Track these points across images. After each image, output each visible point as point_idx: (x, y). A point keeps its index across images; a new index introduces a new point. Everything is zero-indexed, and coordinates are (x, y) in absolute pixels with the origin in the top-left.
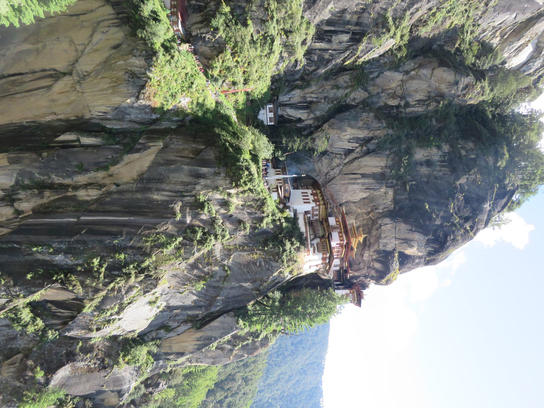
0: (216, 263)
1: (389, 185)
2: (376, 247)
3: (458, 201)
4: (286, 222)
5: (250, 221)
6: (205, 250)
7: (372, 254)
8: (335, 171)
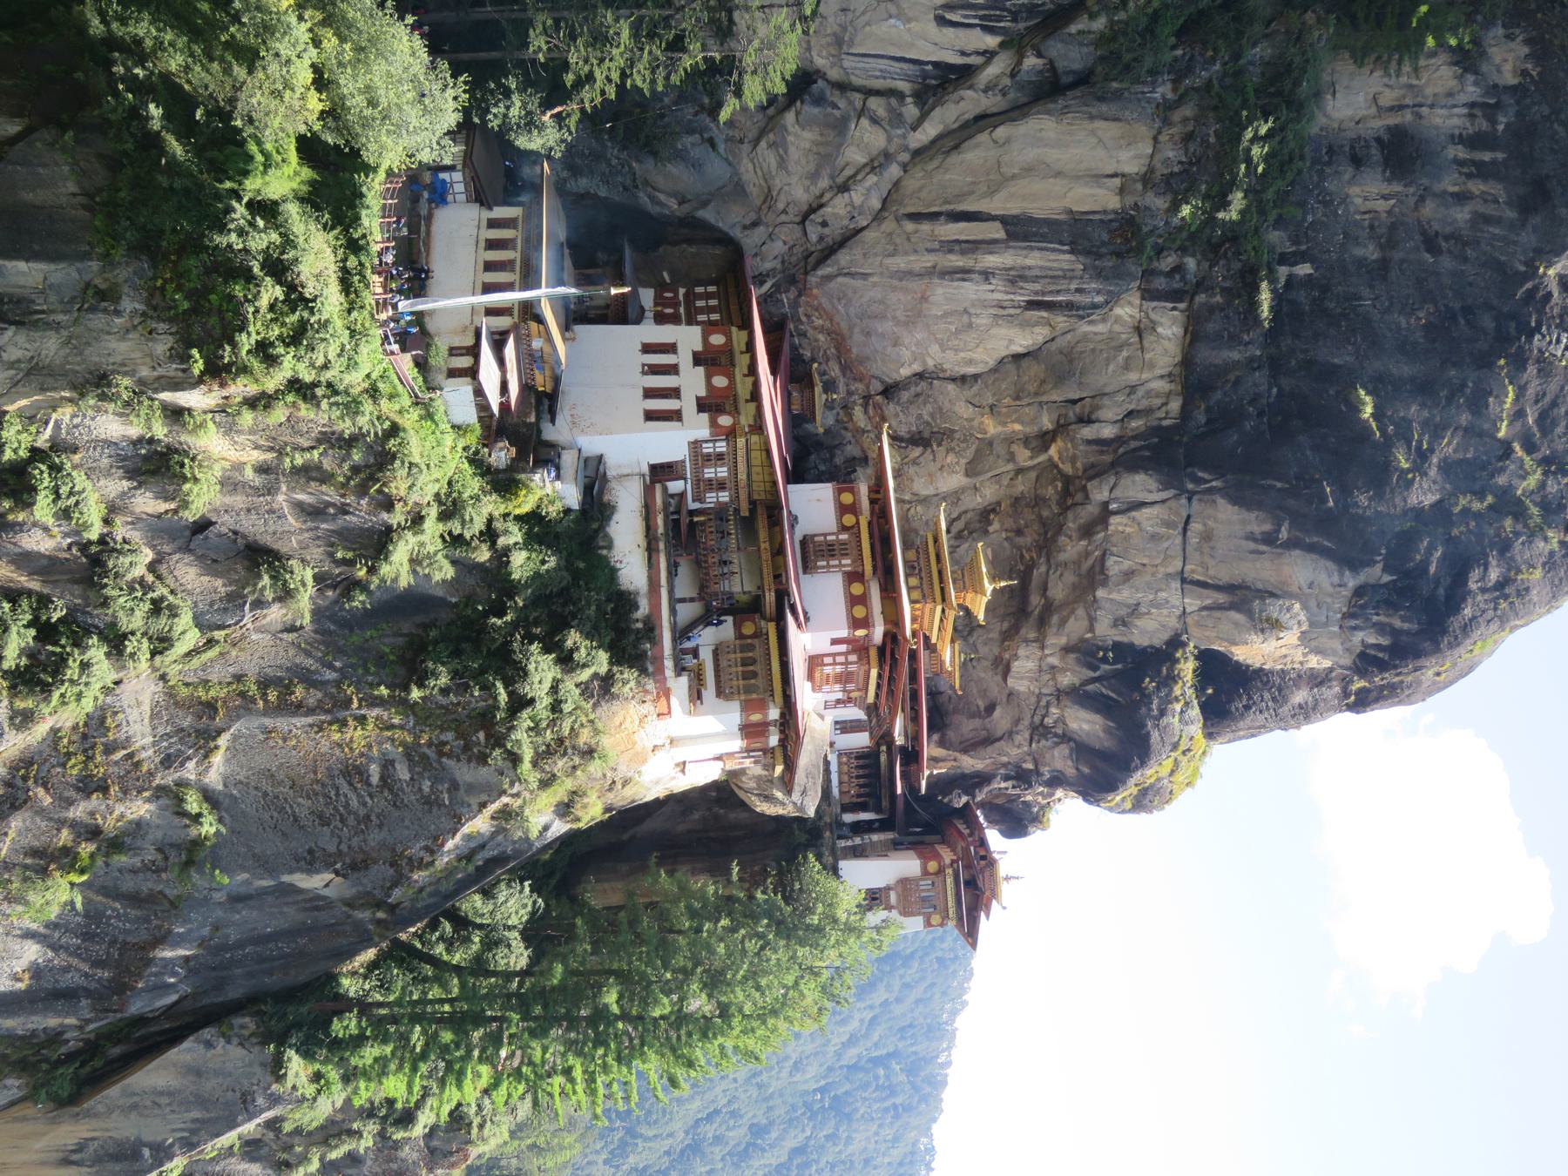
0: (133, 779)
1: (1160, 283)
2: (1076, 627)
4: (531, 541)
5: (316, 553)
6: (61, 714)
8: (857, 196)
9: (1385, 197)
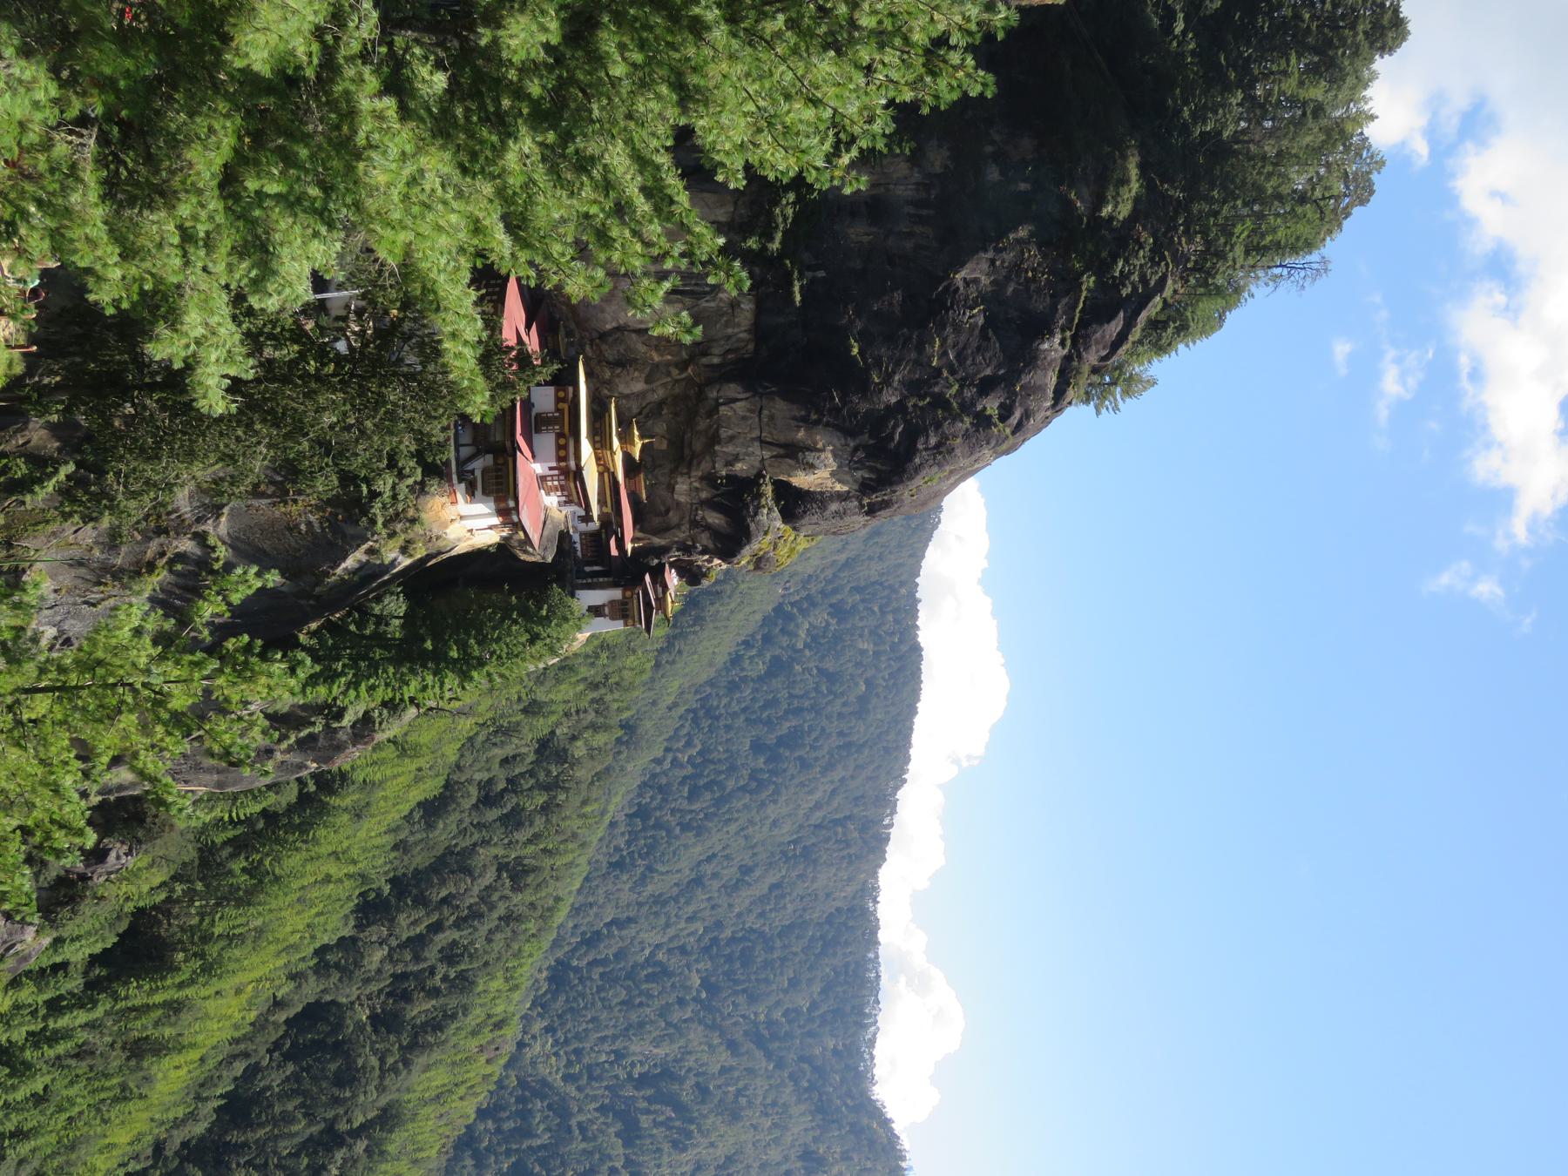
2: (705, 466)
7: (696, 484)
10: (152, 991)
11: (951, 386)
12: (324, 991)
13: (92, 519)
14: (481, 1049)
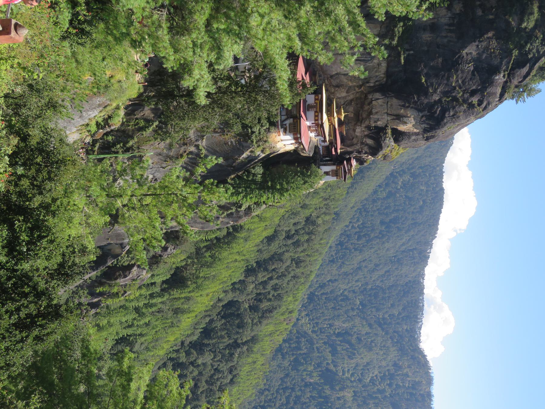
2: (367, 123)
3: (463, 72)
7: (364, 129)
9: (430, 37)
10: (181, 293)
11: (459, 93)
12: (234, 297)
13: (163, 140)
14: (285, 320)
